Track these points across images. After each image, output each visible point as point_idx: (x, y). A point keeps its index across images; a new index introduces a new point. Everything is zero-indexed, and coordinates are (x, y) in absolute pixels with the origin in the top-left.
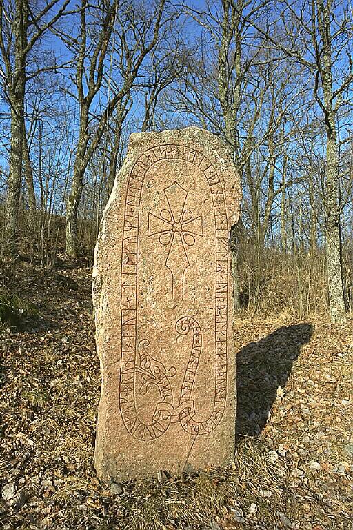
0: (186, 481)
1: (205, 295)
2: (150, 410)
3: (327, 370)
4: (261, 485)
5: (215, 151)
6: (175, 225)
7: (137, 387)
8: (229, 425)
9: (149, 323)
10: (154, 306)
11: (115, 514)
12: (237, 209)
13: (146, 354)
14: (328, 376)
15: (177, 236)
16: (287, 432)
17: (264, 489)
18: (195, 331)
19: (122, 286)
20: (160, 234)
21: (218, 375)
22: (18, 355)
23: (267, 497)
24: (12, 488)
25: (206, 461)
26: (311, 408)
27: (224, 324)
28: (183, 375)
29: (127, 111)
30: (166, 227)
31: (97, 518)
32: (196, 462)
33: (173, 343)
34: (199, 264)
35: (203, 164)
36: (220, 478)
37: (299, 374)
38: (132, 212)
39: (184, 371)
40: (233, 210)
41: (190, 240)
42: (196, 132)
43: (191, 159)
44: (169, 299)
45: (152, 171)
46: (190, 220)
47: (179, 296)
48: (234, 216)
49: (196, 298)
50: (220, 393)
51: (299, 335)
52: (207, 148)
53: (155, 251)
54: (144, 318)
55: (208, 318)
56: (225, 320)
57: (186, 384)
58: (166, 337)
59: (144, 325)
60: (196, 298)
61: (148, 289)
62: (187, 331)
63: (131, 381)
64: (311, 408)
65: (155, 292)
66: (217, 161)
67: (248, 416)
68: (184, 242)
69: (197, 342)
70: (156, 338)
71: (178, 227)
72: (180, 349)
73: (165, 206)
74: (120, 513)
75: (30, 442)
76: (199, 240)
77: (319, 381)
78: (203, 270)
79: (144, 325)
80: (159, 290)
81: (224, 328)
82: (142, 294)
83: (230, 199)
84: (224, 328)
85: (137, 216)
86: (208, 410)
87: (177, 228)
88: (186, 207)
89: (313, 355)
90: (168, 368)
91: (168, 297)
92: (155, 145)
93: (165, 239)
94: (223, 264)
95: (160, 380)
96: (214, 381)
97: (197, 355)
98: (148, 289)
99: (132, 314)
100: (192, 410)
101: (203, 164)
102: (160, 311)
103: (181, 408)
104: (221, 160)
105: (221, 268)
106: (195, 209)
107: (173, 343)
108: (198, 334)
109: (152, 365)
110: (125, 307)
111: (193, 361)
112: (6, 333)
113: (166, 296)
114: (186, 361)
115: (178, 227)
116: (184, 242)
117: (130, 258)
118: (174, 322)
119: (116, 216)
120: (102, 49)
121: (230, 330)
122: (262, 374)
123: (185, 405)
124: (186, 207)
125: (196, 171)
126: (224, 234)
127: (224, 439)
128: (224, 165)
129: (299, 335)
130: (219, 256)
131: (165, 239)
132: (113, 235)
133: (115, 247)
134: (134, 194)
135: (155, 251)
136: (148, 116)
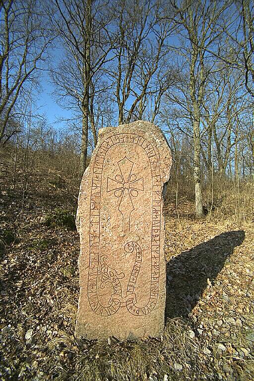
0: (129, 345)
1: (145, 228)
2: (108, 297)
3: (248, 266)
4: (177, 358)
5: (153, 135)
7: (99, 284)
8: (159, 311)
9: (107, 245)
10: (110, 235)
11: (74, 366)
12: (168, 171)
14: (248, 271)
15: (126, 191)
16: (209, 313)
17: (179, 362)
18: (138, 251)
21: (153, 279)
23: (178, 370)
24: (31, 332)
25: (144, 332)
26: (230, 295)
27: (158, 246)
28: (129, 278)
29: (145, 107)
30: (119, 186)
31: (62, 368)
32: (138, 333)
34: (141, 210)
35: (145, 144)
36: (154, 341)
37: (228, 268)
38: (97, 177)
39: (130, 275)
40: (165, 173)
41: (134, 193)
42: (140, 124)
43: (136, 142)
44: (120, 230)
45: (110, 152)
46: (135, 181)
47: (127, 229)
48: (166, 177)
50: (154, 290)
51: (235, 238)
54: (104, 242)
55: (146, 242)
56: (158, 244)
57: (131, 284)
61: (107, 224)
62: (132, 250)
63: (95, 280)
64: (230, 295)
65: (112, 226)
66: (154, 141)
67: (185, 296)
69: (139, 257)
71: (127, 185)
72: (128, 263)
73: (118, 173)
74: (77, 366)
75: (52, 302)
76: (141, 194)
77: (241, 274)
78: (143, 212)
80: (114, 225)
82: (103, 228)
83: (163, 166)
86: (145, 301)
87: (127, 186)
88: (133, 172)
89: (241, 254)
90: (119, 273)
94: (158, 208)
95: (114, 280)
97: (138, 266)
98: (107, 224)
99: (97, 240)
100: (135, 299)
101: (145, 144)
102: (114, 238)
103: (127, 298)
104: (157, 140)
105: (156, 211)
106: (138, 173)
108: (139, 253)
109: (109, 271)
110: (92, 236)
111: (136, 270)
112: (65, 231)
115: (127, 185)
117: (96, 206)
118: (124, 245)
120: (130, 76)
121: (162, 251)
122: (188, 278)
124: (133, 172)
126: (159, 189)
127: (156, 319)
128: (159, 143)
129: (235, 238)
132: (85, 192)
133: (87, 199)
134: (98, 167)
136: (156, 109)
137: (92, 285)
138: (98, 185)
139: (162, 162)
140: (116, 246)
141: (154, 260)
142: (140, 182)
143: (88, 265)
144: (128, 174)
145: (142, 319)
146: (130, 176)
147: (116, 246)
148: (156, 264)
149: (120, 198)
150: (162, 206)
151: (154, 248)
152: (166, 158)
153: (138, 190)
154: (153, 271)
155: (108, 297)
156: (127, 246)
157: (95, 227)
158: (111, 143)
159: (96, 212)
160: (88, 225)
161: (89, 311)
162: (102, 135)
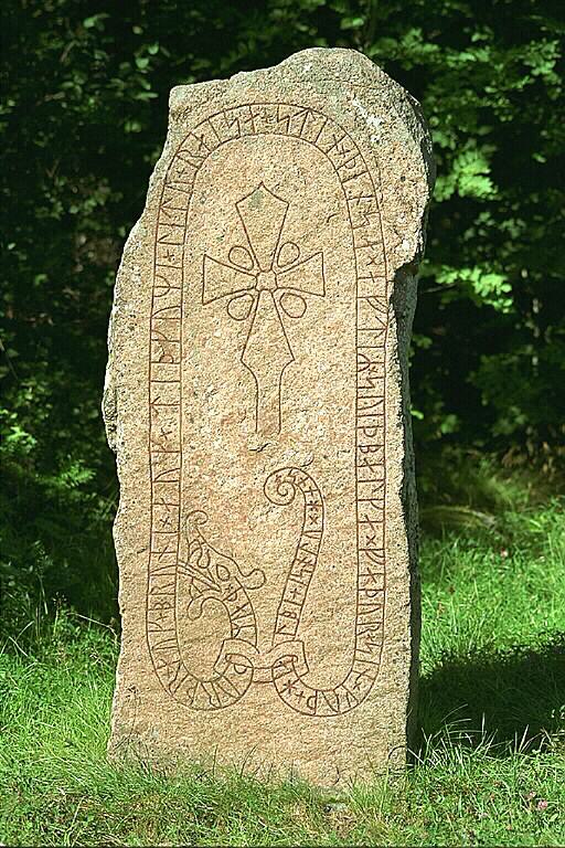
2: (209, 652)
6: (259, 278)
7: (181, 606)
9: (207, 478)
12: (412, 227)
13: (201, 540)
15: (266, 300)
19: (151, 405)
20: (228, 297)
28: (280, 587)
33: (259, 520)
38: (169, 257)
41: (293, 305)
45: (211, 166)
47: (273, 425)
49: (310, 428)
52: (333, 99)
53: (217, 334)
54: (197, 468)
58: (242, 508)
59: (196, 482)
60: (310, 428)
61: (204, 409)
63: (170, 589)
65: (220, 417)
66: (360, 123)
68: (281, 311)
69: (314, 520)
70: (221, 508)
71: (267, 280)
78: (324, 368)
79: (196, 482)
80: (227, 411)
81: (379, 494)
83: (394, 208)
84: (379, 494)
85: (179, 265)
87: (265, 282)
88: (286, 236)
90: (247, 571)
91: (248, 426)
92: (216, 111)
93: (239, 307)
94: (373, 354)
95: (229, 591)
96: (354, 606)
97: (311, 547)
106: (306, 238)
107: (259, 520)
108: (314, 505)
109: (213, 562)
110: (157, 448)
111: (303, 563)
113: (244, 423)
114: (286, 559)
115: (267, 280)
116: (281, 311)
119: (137, 268)
123: (283, 649)
124: (286, 236)
126: (382, 288)
128: (380, 130)
130: (362, 339)
131: (239, 307)
132: (131, 306)
133: (137, 329)
134: (172, 221)
135: (217, 334)
137: (163, 606)
138: (173, 283)
139: (389, 195)
140: (235, 483)
141: (366, 531)
142: (312, 267)
143: (146, 543)
144: (269, 242)
145: (324, 731)
147: (235, 483)
148: (372, 546)
149: (246, 323)
150: (389, 349)
151: (365, 490)
152: (403, 179)
153: (305, 295)
155: (209, 652)
156: (271, 484)
160: (144, 413)
161: (152, 689)
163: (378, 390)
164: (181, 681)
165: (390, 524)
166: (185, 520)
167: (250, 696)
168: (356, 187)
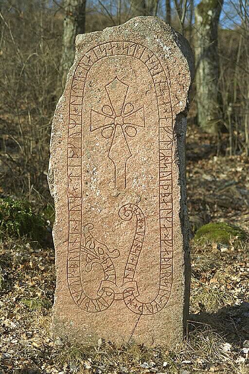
1: (148, 183)
2: (95, 286)
6: (116, 119)
9: (93, 209)
12: (184, 95)
13: (91, 237)
19: (69, 177)
20: (102, 128)
21: (163, 260)
22: (28, 268)
33: (117, 227)
34: (141, 153)
35: (145, 55)
38: (75, 110)
39: (127, 253)
41: (131, 131)
45: (92, 71)
47: (122, 184)
48: (181, 103)
49: (139, 186)
52: (148, 39)
53: (97, 144)
54: (89, 204)
57: (130, 266)
58: (109, 222)
59: (89, 211)
60: (139, 186)
61: (92, 179)
65: (99, 181)
66: (160, 49)
68: (125, 134)
69: (141, 228)
70: (100, 222)
71: (119, 120)
72: (125, 234)
73: (105, 101)
78: (145, 159)
79: (89, 211)
82: (87, 183)
83: (176, 87)
85: (80, 114)
87: (119, 121)
88: (127, 100)
90: (111, 250)
91: (111, 186)
92: (96, 45)
93: (107, 132)
94: (167, 153)
96: (159, 266)
98: (92, 179)
101: (145, 55)
103: (124, 287)
107: (117, 227)
108: (141, 221)
110: (71, 195)
111: (136, 246)
112: (25, 248)
113: (110, 185)
114: (129, 245)
115: (119, 120)
116: (125, 134)
117: (75, 152)
119: (61, 116)
123: (127, 285)
124: (127, 100)
125: (137, 64)
126: (169, 123)
130: (162, 145)
131: (107, 132)
132: (59, 133)
133: (62, 143)
135: (97, 144)
137: (75, 266)
138: (77, 122)
139: (173, 81)
140: (106, 211)
141: (164, 232)
142: (140, 114)
143: (67, 237)
144: (120, 103)
146: (124, 106)
147: (106, 211)
148: (166, 238)
149: (110, 140)
150: (174, 150)
152: (179, 74)
153: (136, 127)
154: (163, 249)
155: (95, 286)
156: (122, 211)
157: (76, 184)
158: (93, 58)
159: (76, 162)
160: (65, 180)
162: (81, 46)
163: (168, 169)
164: (83, 300)
165: (175, 229)
166: (83, 225)
167: (114, 305)
168: (157, 78)
